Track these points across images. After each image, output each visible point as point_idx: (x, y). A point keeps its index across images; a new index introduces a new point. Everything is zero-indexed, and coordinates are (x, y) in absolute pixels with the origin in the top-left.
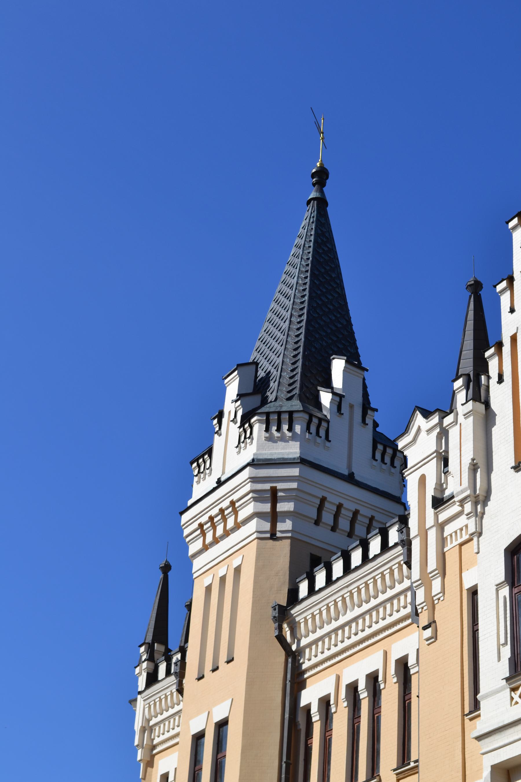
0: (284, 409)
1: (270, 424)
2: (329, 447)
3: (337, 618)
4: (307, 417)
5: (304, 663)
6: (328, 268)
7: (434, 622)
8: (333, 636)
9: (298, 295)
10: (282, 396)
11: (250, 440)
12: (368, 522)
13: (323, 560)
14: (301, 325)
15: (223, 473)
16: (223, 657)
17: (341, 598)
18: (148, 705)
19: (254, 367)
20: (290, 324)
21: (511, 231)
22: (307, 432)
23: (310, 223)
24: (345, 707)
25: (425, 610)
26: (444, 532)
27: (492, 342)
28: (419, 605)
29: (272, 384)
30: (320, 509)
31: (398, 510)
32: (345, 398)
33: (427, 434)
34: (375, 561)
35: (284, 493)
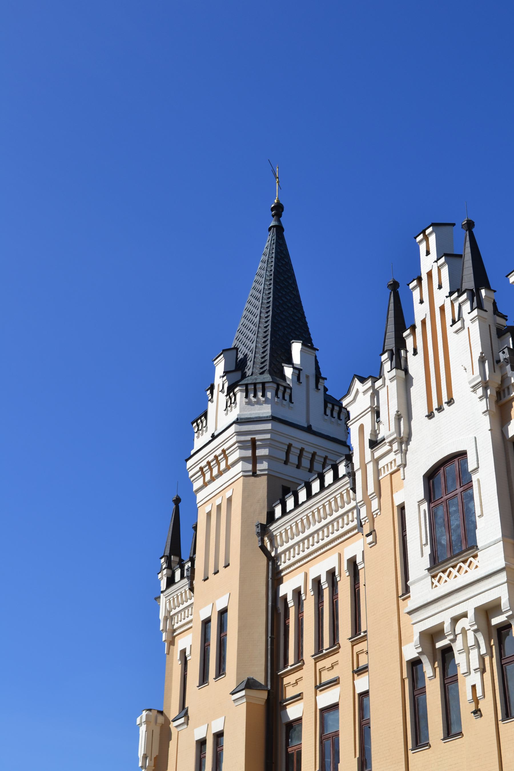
0: (258, 381)
1: (249, 392)
2: (292, 408)
3: (304, 532)
4: (275, 386)
5: (281, 565)
6: (286, 276)
7: (374, 531)
8: (301, 545)
9: (265, 297)
10: (256, 371)
11: (234, 404)
12: (323, 460)
13: (292, 489)
14: (268, 319)
15: (216, 429)
16: (222, 563)
17: (305, 517)
18: (168, 601)
19: (235, 351)
20: (260, 319)
21: (418, 244)
22: (276, 397)
23: (272, 244)
24: (312, 595)
25: (367, 523)
26: (379, 465)
27: (408, 325)
28: (362, 519)
29: (248, 363)
30: (288, 453)
31: (346, 451)
32: (303, 371)
33: (364, 394)
34: (329, 488)
35: (260, 442)
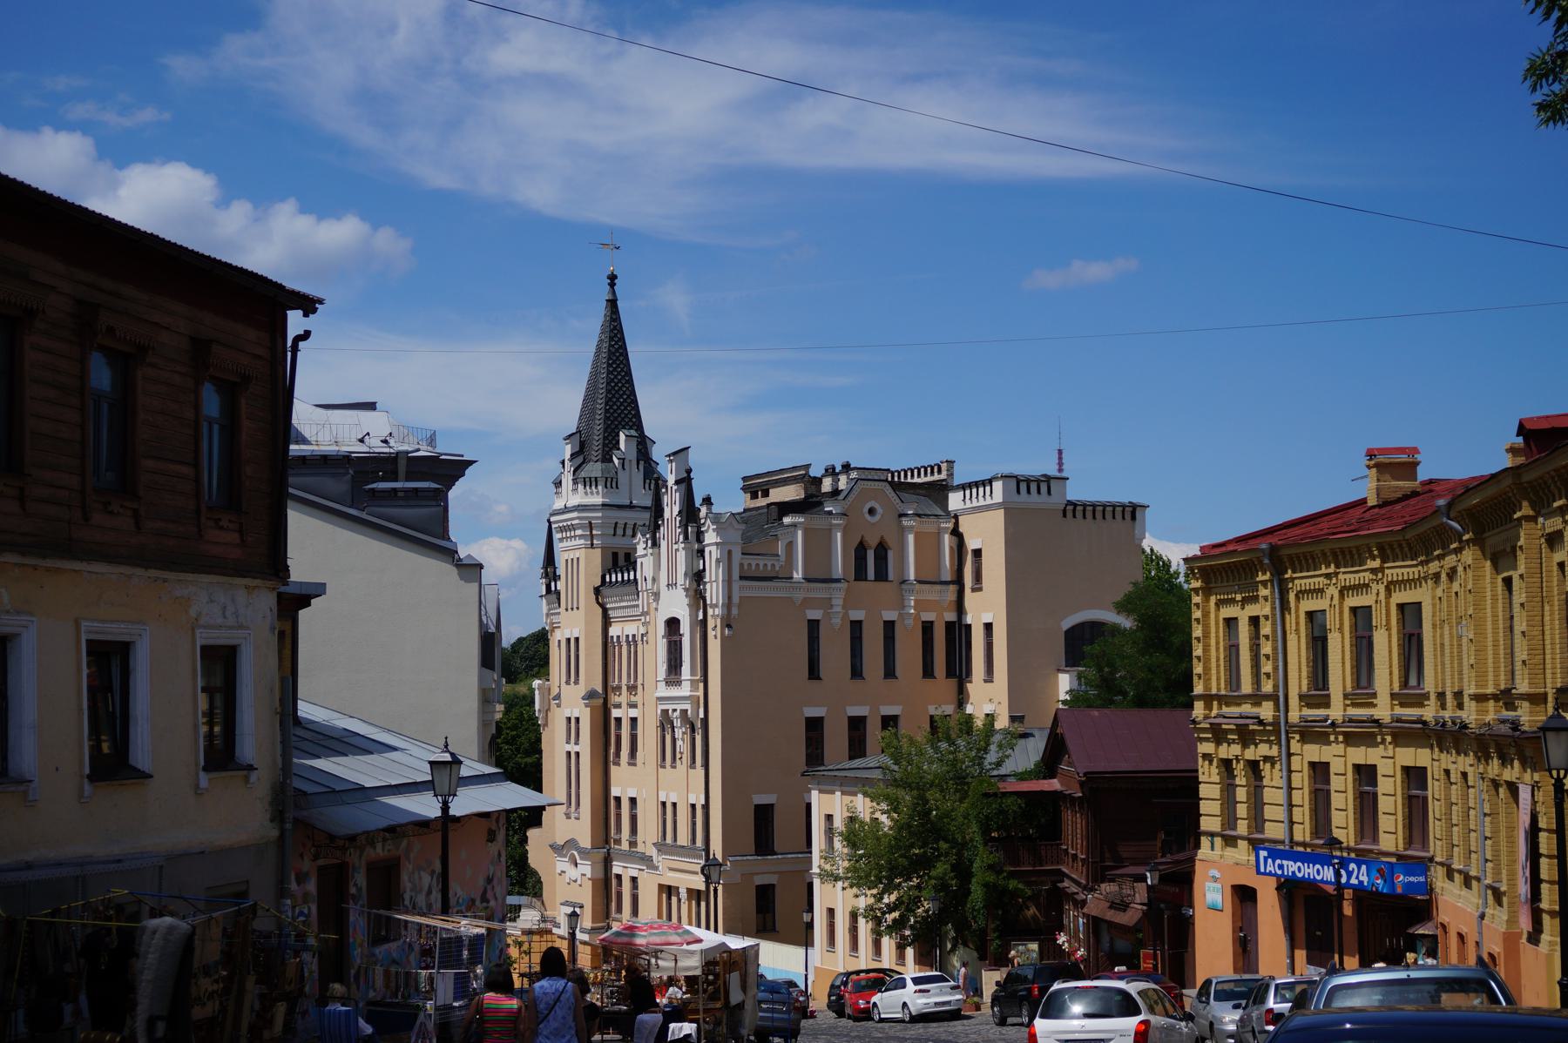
0: (593, 475)
16: (575, 606)
30: (615, 528)
